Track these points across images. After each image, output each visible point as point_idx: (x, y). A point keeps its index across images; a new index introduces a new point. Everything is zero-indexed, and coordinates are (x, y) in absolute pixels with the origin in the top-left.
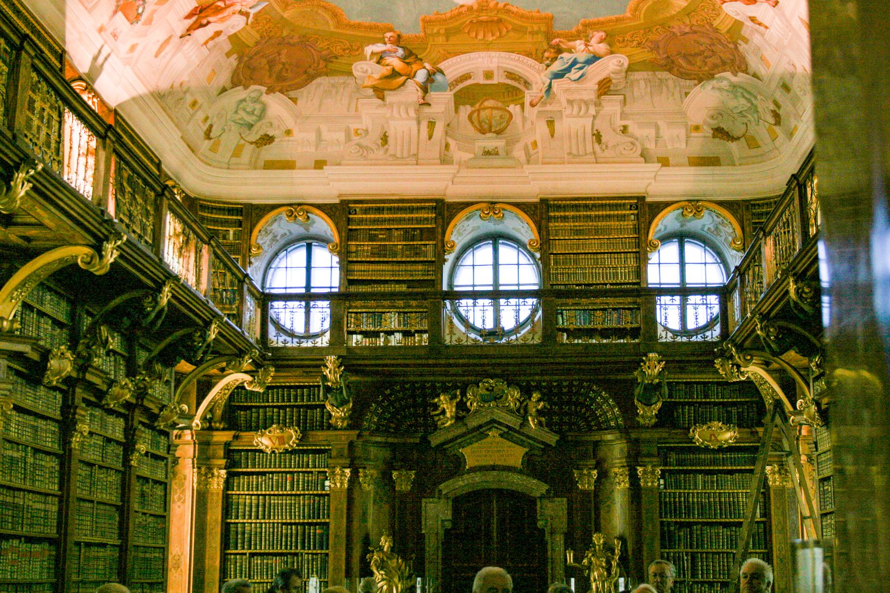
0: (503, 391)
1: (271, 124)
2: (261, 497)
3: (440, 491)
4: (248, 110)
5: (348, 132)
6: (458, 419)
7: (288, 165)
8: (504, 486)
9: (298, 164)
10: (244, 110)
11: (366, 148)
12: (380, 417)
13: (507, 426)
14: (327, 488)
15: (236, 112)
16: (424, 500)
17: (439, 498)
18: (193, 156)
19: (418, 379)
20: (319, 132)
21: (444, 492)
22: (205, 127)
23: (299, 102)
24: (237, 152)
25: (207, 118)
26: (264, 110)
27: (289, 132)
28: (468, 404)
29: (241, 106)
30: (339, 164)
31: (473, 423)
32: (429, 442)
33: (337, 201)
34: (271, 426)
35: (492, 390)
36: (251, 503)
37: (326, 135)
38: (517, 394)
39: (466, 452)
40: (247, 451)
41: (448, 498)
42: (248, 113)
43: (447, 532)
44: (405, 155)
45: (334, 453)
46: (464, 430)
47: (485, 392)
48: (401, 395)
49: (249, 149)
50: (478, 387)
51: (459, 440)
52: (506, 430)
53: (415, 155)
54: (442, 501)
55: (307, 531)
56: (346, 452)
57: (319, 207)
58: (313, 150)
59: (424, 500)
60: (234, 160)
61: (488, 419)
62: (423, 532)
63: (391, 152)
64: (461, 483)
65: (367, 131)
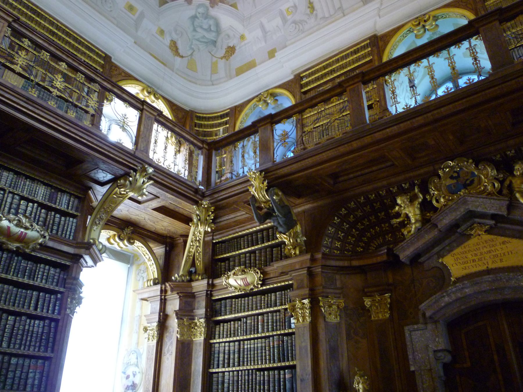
0: (473, 173)
1: (229, 36)
2: (237, 343)
3: (424, 314)
4: (206, 27)
5: (281, 14)
6: (425, 221)
7: (251, 65)
8: (509, 295)
9: (257, 62)
10: (201, 27)
11: (301, 22)
12: (343, 241)
13: (493, 217)
14: (293, 326)
15: (195, 30)
16: (406, 328)
17: (426, 323)
18: (166, 68)
19: (369, 187)
20: (262, 27)
21: (428, 314)
22: (167, 42)
23: (239, 6)
24: (214, 70)
25: (162, 32)
26: (217, 25)
27: (242, 37)
28: (434, 202)
29: (196, 23)
30: (285, 47)
31: (445, 221)
32: (397, 257)
33: (292, 77)
34: (233, 269)
35: (459, 176)
36: (229, 350)
37: (269, 26)
38: (492, 172)
39: (448, 260)
40: (225, 299)
41: (436, 322)
42: (205, 30)
43: (446, 366)
44: (332, 12)
45: (295, 286)
46: (433, 234)
47: (449, 182)
48: (359, 213)
49: (221, 63)
50: (439, 177)
51: (436, 249)
52: (492, 222)
53: (341, 8)
54: (430, 326)
55: (277, 376)
56: (306, 282)
57: (280, 87)
58: (263, 44)
59: (406, 328)
60: (215, 77)
61: (462, 211)
62: (412, 368)
63: (320, 15)
64: (447, 299)
65: (295, 7)
